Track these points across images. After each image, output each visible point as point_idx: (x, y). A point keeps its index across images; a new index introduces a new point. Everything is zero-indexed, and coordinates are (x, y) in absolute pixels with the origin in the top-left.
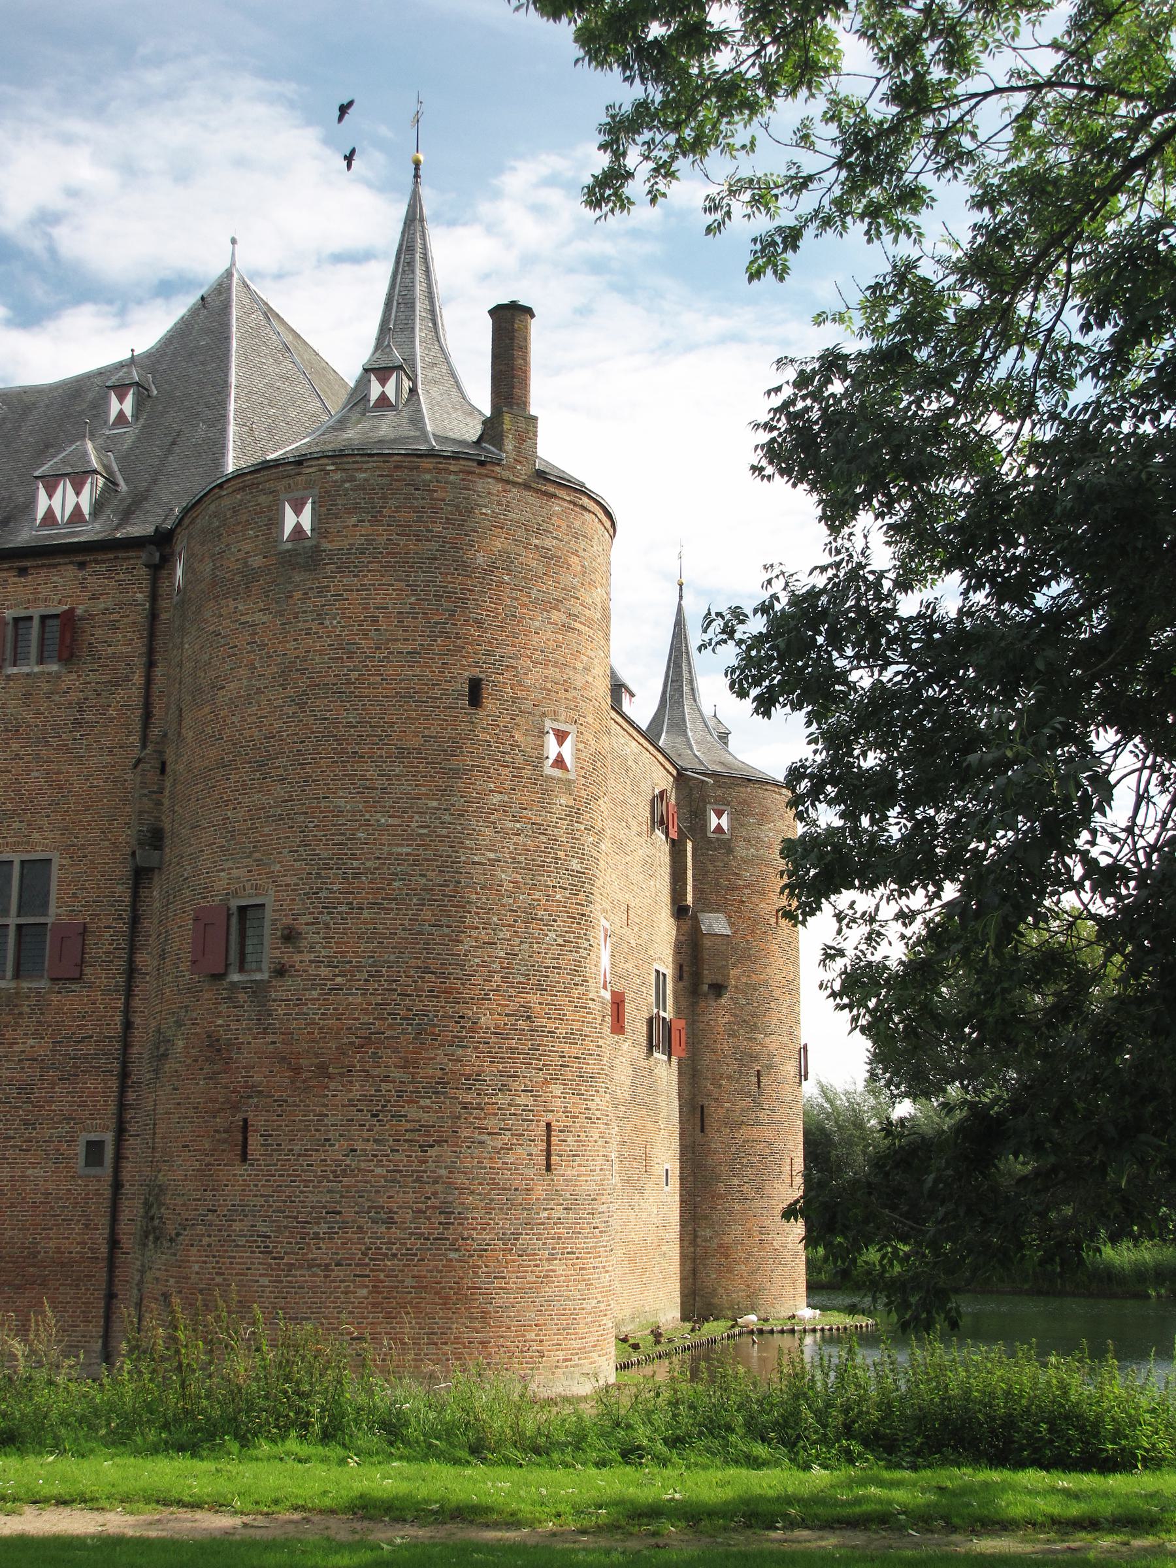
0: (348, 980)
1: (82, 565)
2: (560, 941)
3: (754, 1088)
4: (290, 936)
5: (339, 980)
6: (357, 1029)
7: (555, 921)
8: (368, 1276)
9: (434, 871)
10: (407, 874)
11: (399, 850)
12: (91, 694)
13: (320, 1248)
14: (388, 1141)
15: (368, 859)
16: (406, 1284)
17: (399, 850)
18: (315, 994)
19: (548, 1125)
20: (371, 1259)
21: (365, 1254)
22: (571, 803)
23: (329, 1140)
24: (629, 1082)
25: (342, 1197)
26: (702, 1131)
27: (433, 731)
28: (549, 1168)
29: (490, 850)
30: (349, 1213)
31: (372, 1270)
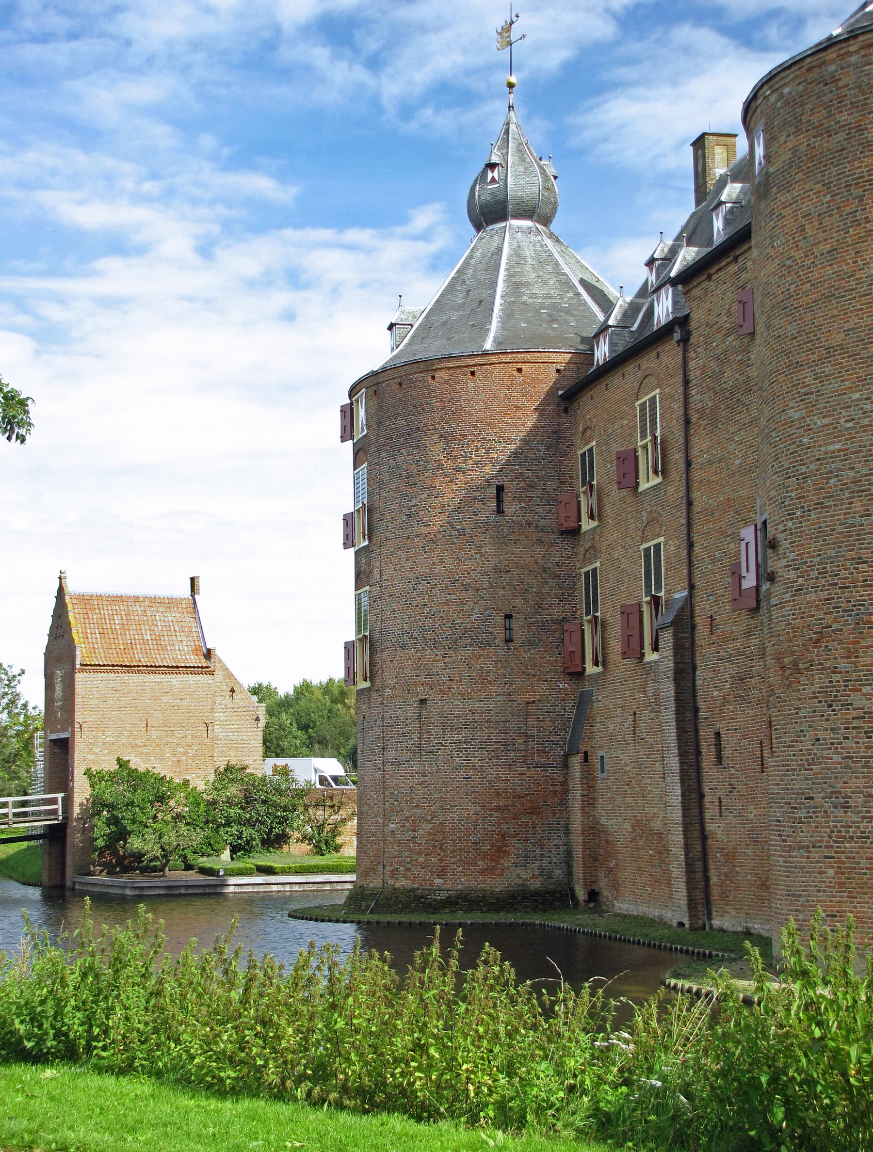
0: (806, 580)
6: (815, 625)
8: (833, 857)
9: (860, 462)
10: (839, 470)
11: (831, 448)
13: (802, 832)
14: (840, 729)
15: (811, 462)
16: (862, 865)
17: (831, 448)
20: (835, 842)
21: (830, 837)
23: (802, 731)
25: (814, 783)
27: (851, 324)
30: (818, 800)
31: (836, 852)
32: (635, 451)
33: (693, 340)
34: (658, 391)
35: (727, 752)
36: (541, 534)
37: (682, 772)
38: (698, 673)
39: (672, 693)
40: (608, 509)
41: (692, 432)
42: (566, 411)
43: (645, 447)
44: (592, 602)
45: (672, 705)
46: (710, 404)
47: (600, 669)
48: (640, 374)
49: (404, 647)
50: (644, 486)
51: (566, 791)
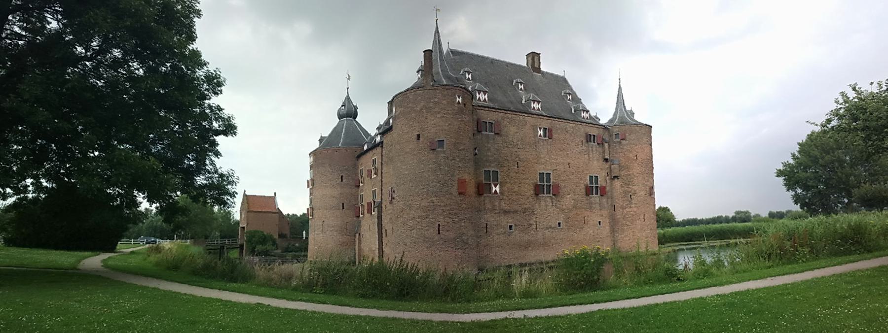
3: (630, 199)
19: (439, 225)
26: (614, 210)
28: (439, 233)
33: (384, 146)
35: (388, 234)
37: (379, 238)
42: (357, 160)
44: (362, 201)
47: (363, 216)
49: (319, 209)
50: (372, 177)
51: (355, 241)
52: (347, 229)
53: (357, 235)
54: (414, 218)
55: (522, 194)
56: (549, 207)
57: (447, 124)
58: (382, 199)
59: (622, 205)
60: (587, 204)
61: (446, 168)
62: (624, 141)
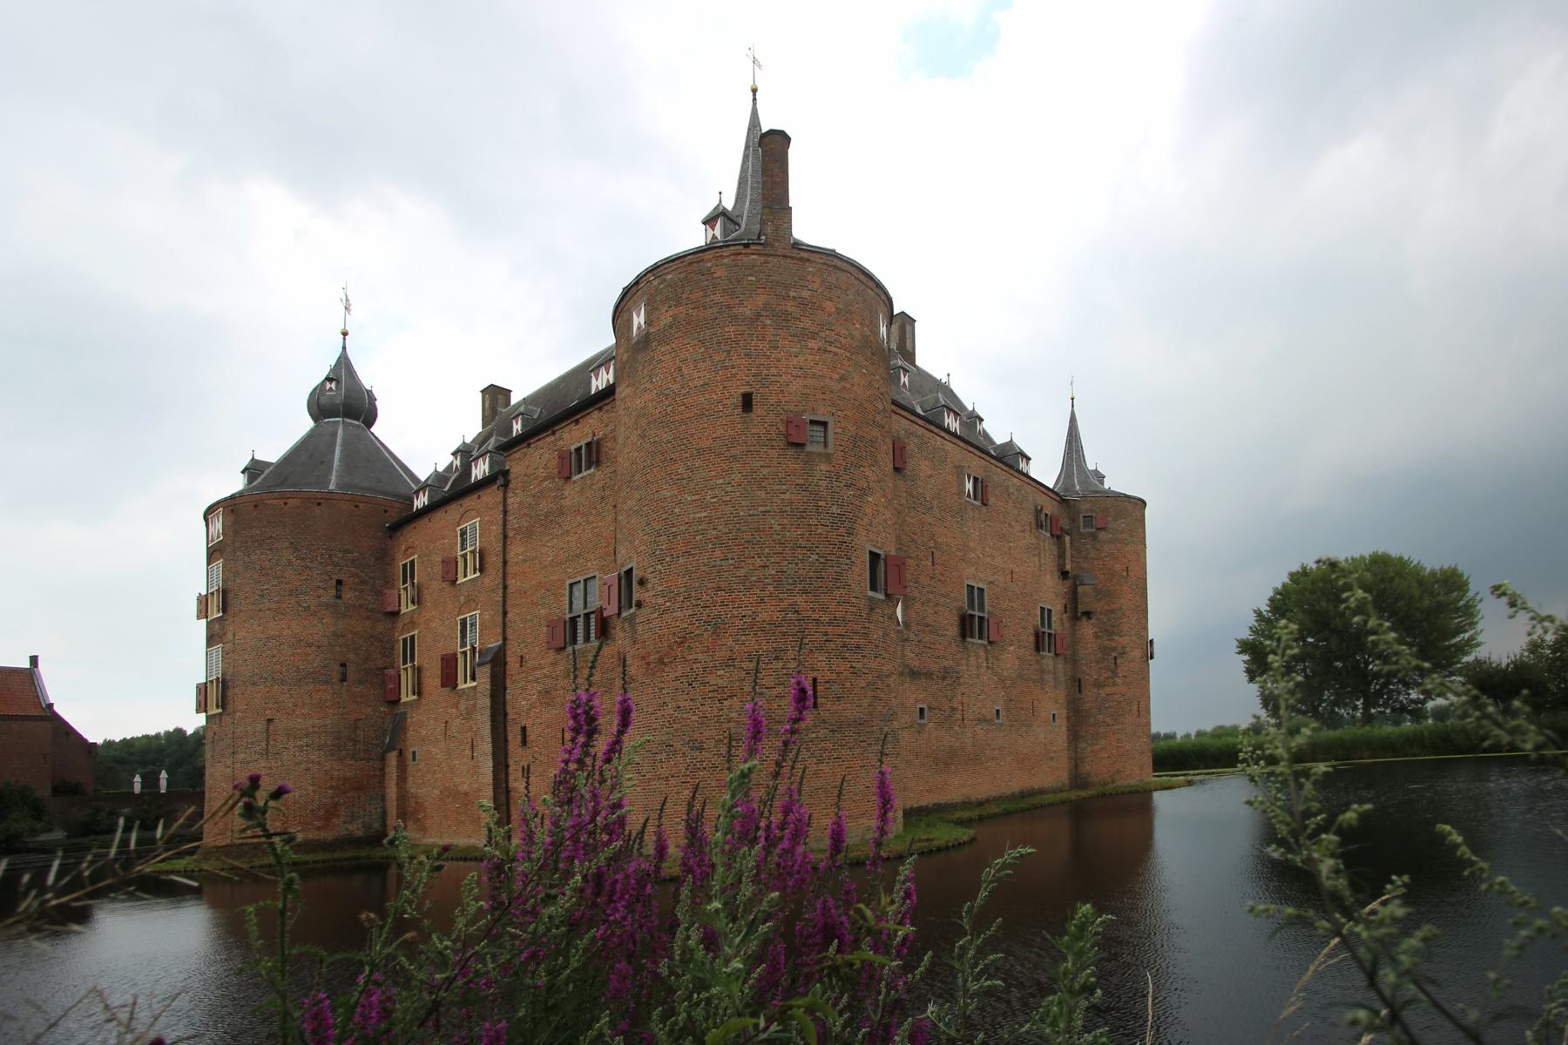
1: (600, 409)
2: (822, 560)
3: (1112, 666)
4: (642, 582)
5: (668, 604)
7: (816, 547)
10: (704, 529)
11: (699, 515)
12: (608, 480)
17: (699, 515)
18: (656, 615)
22: (829, 468)
24: (1016, 667)
29: (762, 506)
32: (456, 558)
34: (479, 519)
36: (369, 613)
38: (508, 692)
39: (489, 704)
40: (427, 596)
41: (509, 543)
43: (464, 556)
44: (408, 653)
45: (488, 712)
46: (526, 524)
47: (415, 697)
48: (462, 510)
51: (383, 775)
52: (355, 742)
53: (392, 758)
54: (732, 659)
55: (940, 632)
56: (982, 670)
57: (836, 376)
58: (505, 639)
59: (1096, 680)
60: (1037, 670)
61: (835, 509)
62: (1103, 533)
